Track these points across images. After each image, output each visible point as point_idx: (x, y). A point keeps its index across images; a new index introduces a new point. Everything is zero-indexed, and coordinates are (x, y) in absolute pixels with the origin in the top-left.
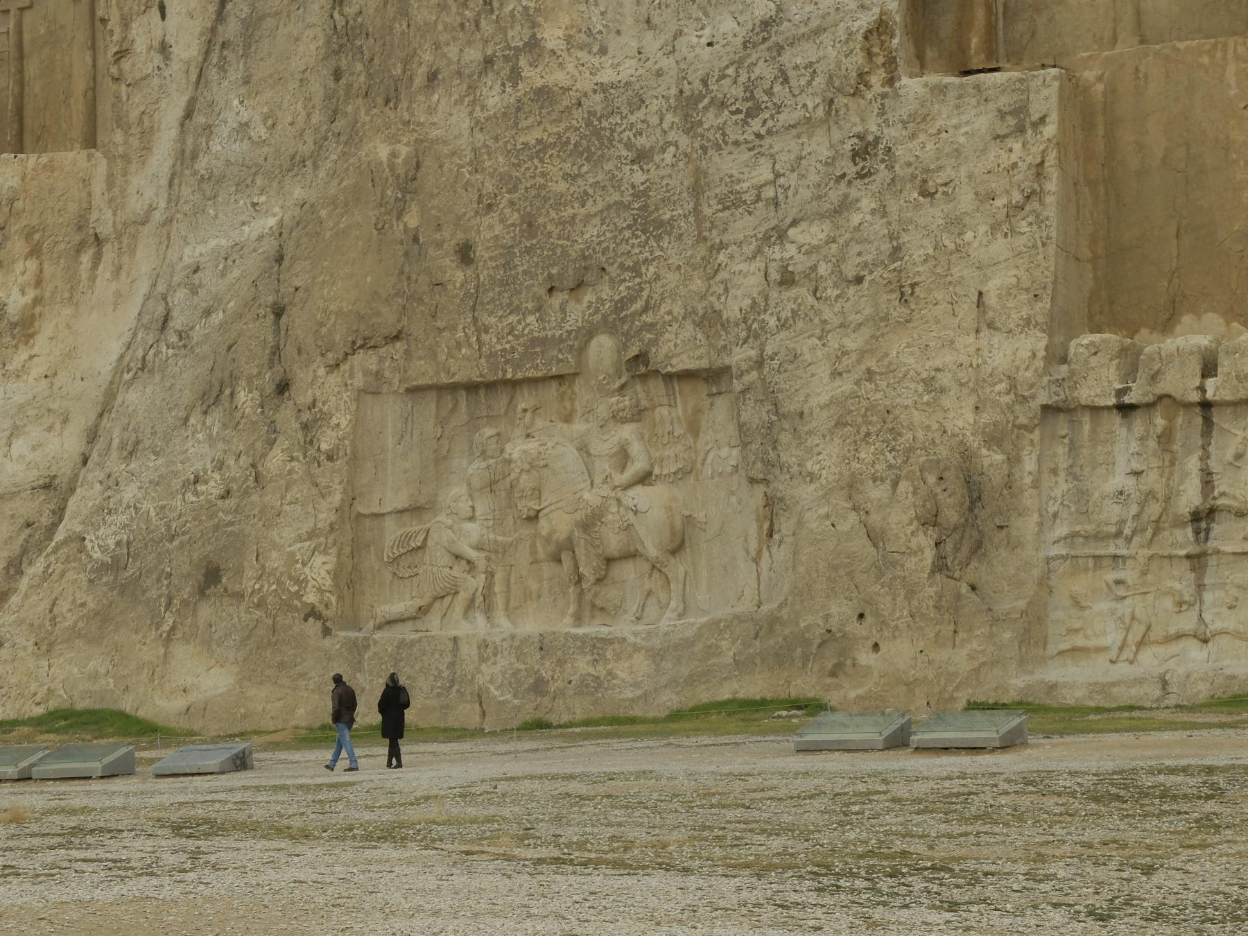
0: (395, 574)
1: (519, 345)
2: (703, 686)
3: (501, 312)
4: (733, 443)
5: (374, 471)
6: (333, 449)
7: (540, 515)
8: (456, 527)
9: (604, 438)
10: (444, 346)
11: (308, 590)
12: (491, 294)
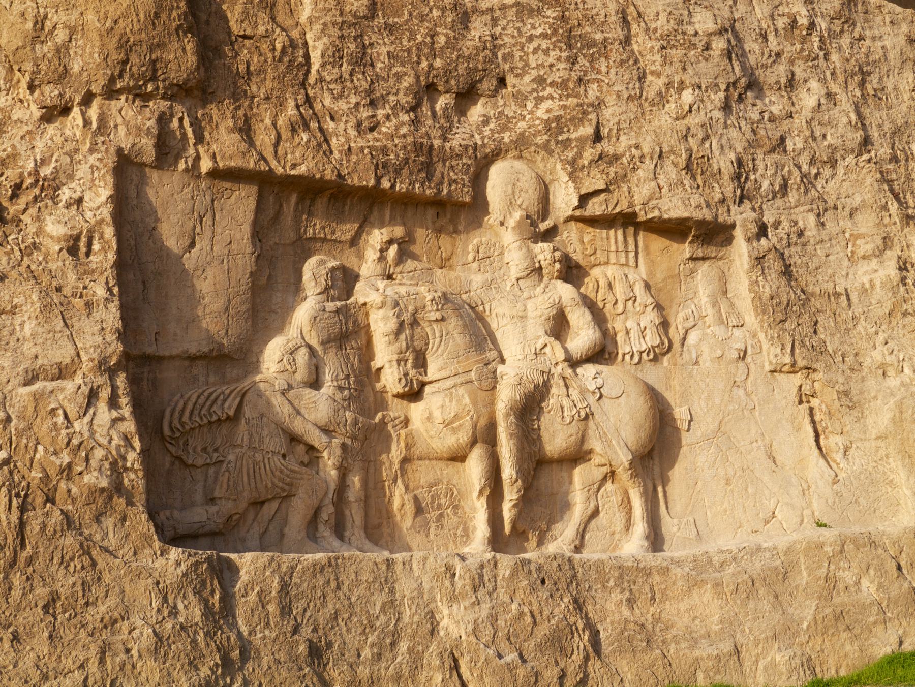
0: (178, 458)
2: (844, 635)
3: (353, 99)
4: (733, 321)
5: (141, 286)
6: (77, 238)
7: (427, 389)
9: (526, 295)
10: (268, 121)
11: (94, 463)
12: (336, 70)
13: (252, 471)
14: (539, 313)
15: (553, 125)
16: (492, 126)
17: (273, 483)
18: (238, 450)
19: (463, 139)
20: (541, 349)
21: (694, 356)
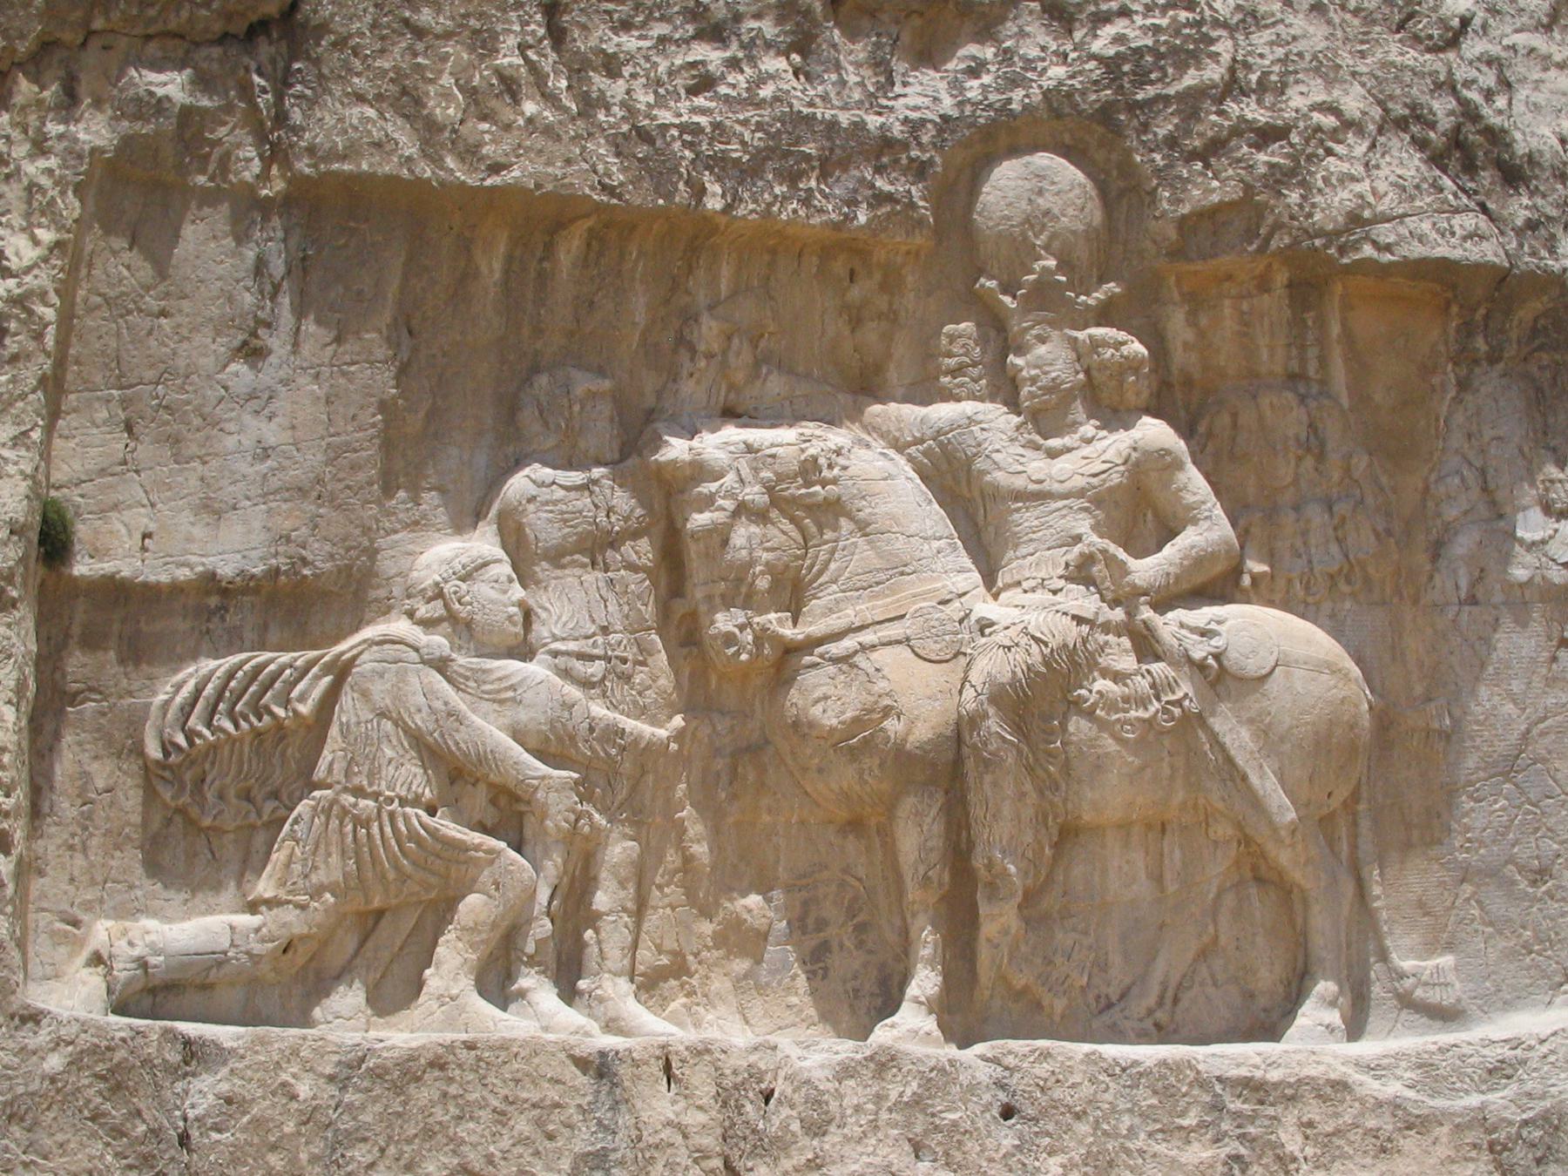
1: (744, 123)
3: (660, 29)
8: (462, 661)
10: (447, 80)
13: (350, 838)
14: (1079, 482)
15: (1126, 68)
16: (986, 79)
17: (397, 867)
18: (317, 794)
19: (916, 108)
20: (1079, 567)
21: (1464, 583)
